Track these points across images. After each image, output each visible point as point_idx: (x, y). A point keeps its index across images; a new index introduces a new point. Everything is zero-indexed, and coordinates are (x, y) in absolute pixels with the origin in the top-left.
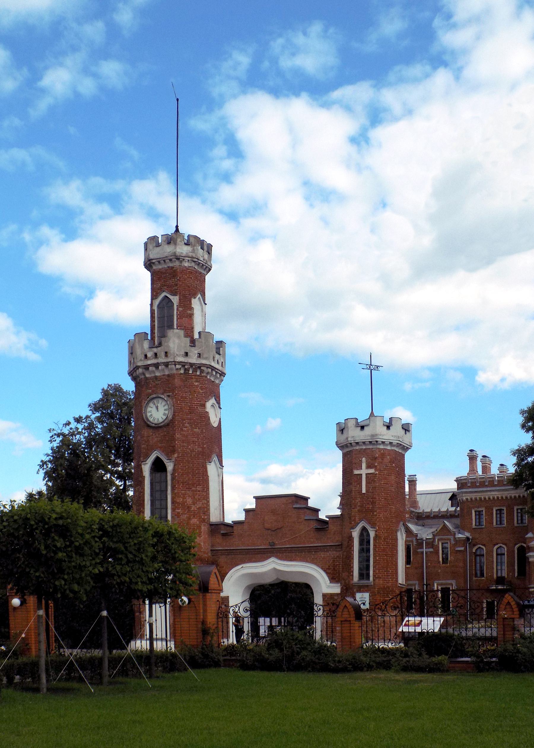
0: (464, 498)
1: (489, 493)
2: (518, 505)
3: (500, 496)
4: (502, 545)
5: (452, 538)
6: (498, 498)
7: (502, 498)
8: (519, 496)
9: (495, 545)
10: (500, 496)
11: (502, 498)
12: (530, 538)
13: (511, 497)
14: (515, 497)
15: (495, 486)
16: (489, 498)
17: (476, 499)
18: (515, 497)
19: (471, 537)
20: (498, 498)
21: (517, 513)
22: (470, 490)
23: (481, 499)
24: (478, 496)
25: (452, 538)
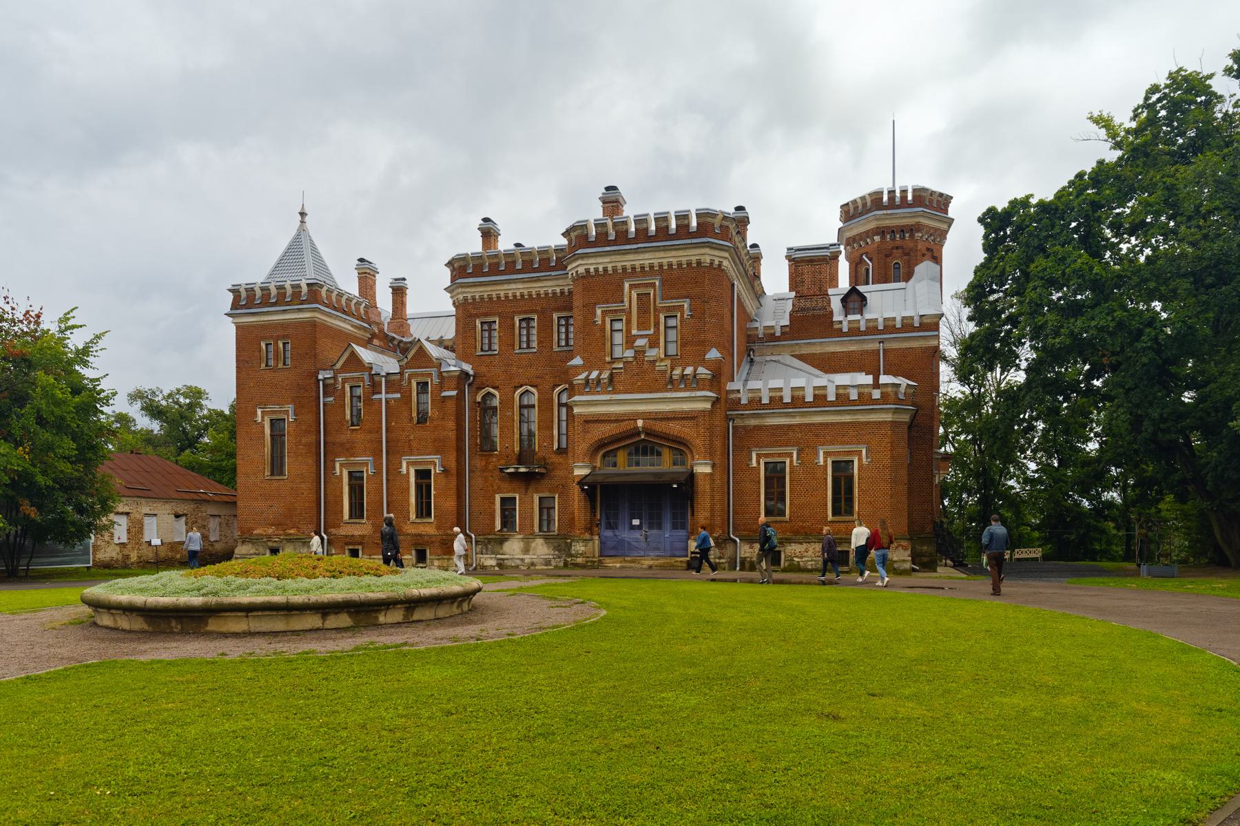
0: (461, 297)
1: (506, 287)
2: (558, 309)
3: (526, 292)
4: (529, 388)
5: (434, 371)
6: (522, 296)
7: (530, 295)
8: (562, 293)
9: (516, 388)
10: (526, 292)
11: (530, 295)
12: (576, 367)
13: (547, 294)
14: (554, 293)
15: (519, 272)
16: (507, 297)
17: (482, 298)
18: (554, 293)
19: (471, 372)
20: (522, 296)
21: (559, 325)
22: (471, 280)
23: (490, 298)
24: (485, 292)
25: (434, 371)
